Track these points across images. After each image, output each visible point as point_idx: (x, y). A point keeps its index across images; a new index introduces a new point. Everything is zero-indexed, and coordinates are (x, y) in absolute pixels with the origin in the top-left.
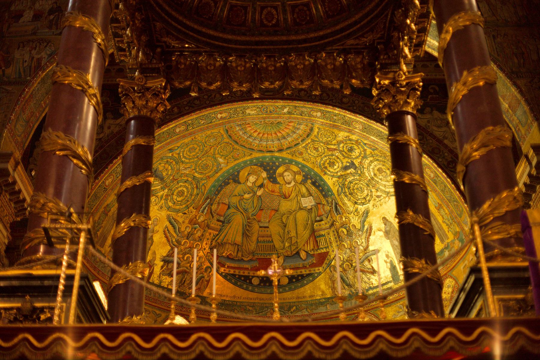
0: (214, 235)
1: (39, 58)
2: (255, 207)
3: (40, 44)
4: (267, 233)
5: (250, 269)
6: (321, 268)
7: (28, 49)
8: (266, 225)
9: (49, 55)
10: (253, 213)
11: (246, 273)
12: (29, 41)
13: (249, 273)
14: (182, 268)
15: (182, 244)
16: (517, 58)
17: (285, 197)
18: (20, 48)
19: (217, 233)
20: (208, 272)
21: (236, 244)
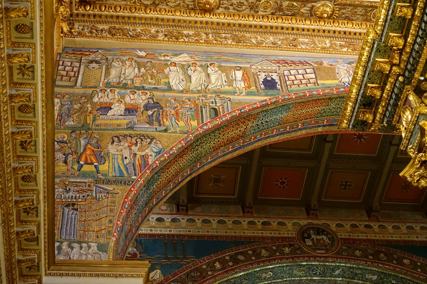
1: (143, 156)
3: (142, 140)
7: (126, 144)
9: (156, 152)
12: (125, 136)
18: (115, 143)
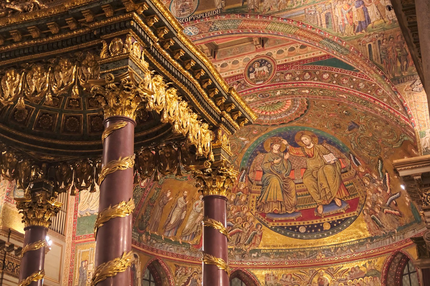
4: (303, 188)
5: (295, 220)
6: (355, 212)
8: (300, 181)
11: (293, 224)
13: (295, 224)
14: (235, 229)
15: (231, 209)
16: (400, 61)
17: (309, 157)
19: (259, 195)
20: (259, 228)
21: (278, 201)
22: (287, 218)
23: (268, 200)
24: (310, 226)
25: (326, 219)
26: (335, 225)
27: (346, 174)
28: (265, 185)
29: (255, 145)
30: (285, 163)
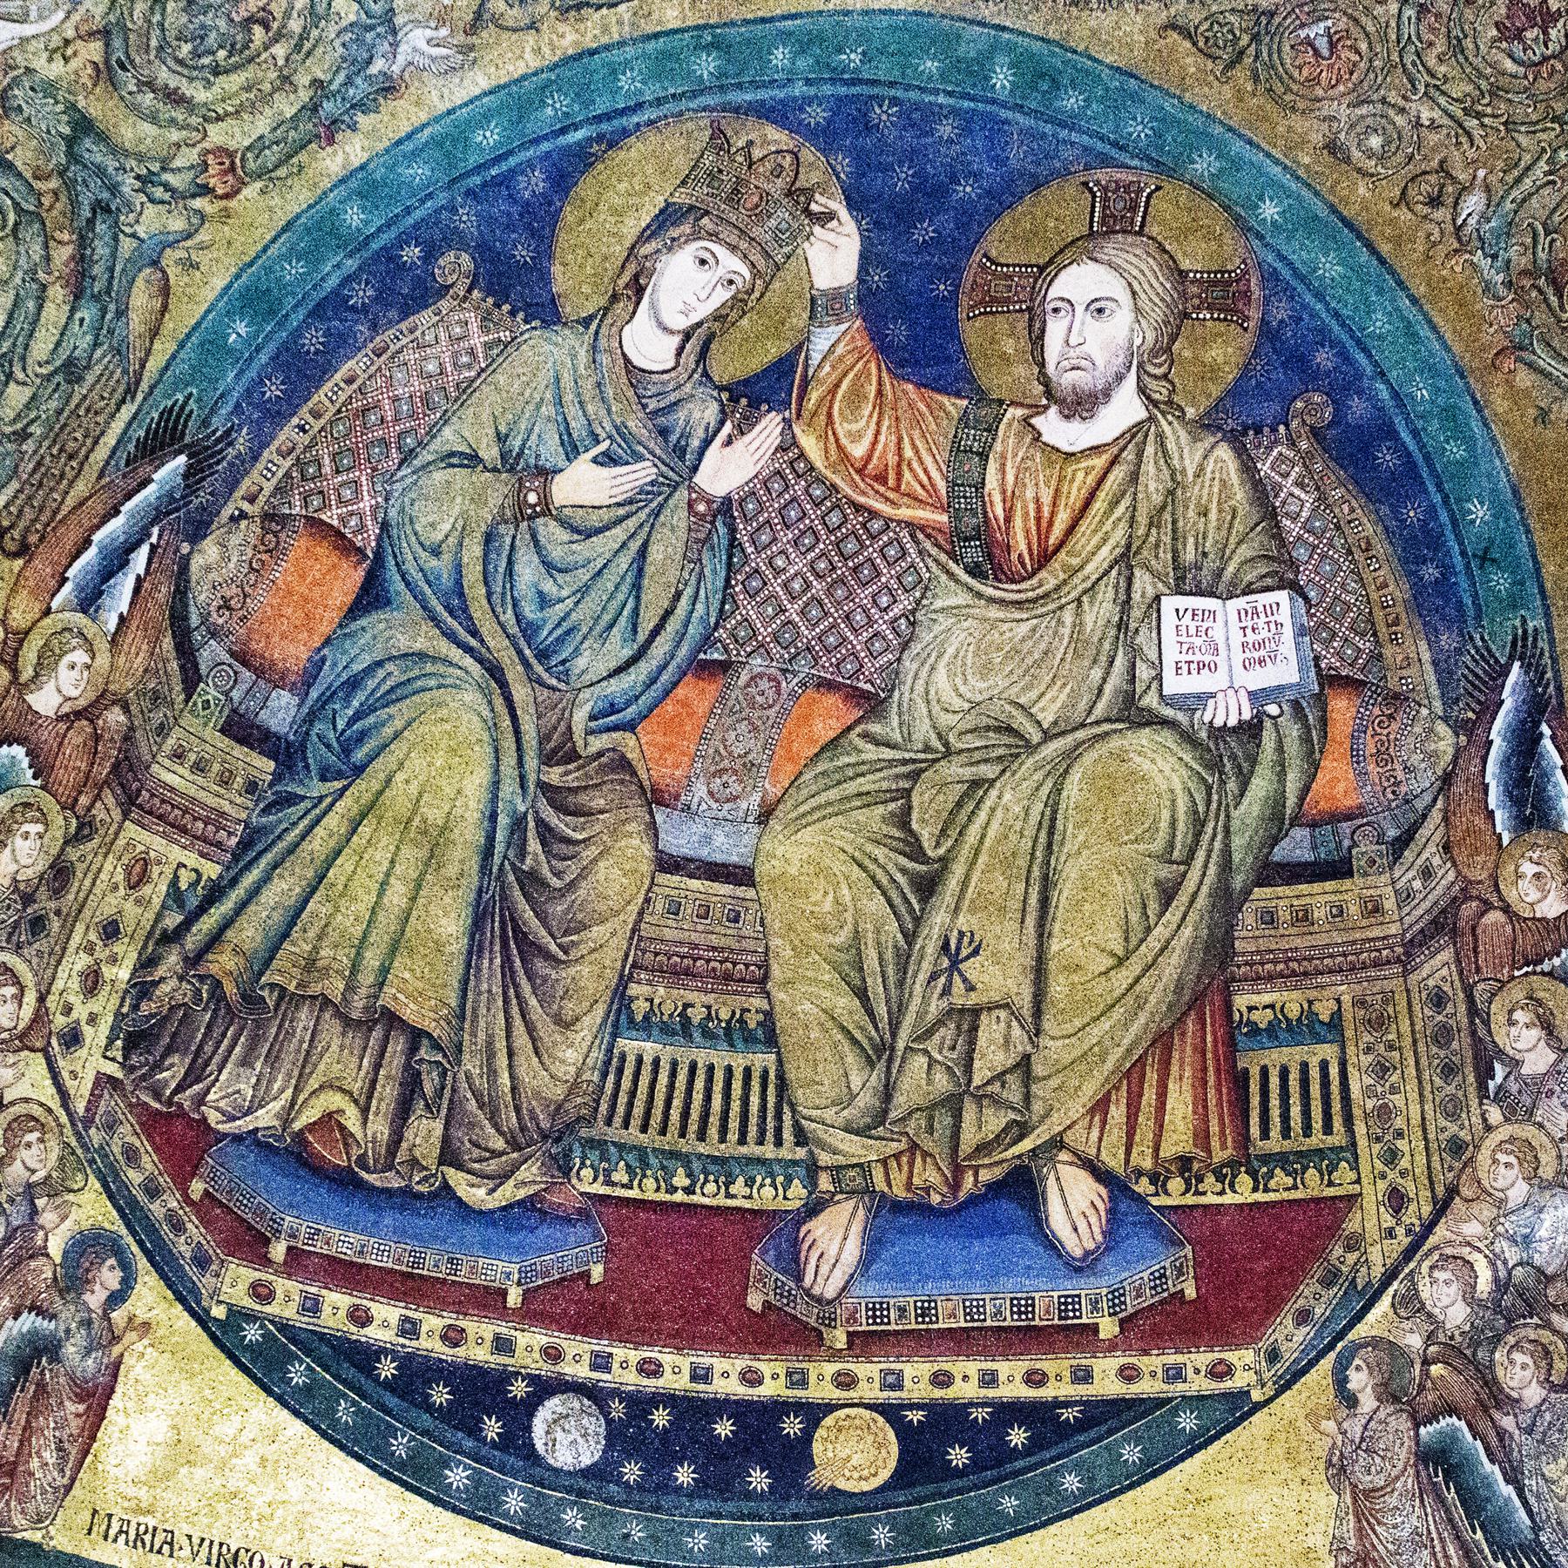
0: (175, 895)
2: (646, 626)
5: (514, 1298)
6: (1242, 1357)
8: (725, 847)
10: (616, 687)
13: (503, 1345)
19: (212, 870)
21: (392, 1020)
22: (433, 1265)
23: (283, 973)
24: (660, 1418)
25: (867, 1371)
26: (959, 1456)
27: (1319, 896)
28: (316, 754)
29: (489, 137)
30: (666, 549)
